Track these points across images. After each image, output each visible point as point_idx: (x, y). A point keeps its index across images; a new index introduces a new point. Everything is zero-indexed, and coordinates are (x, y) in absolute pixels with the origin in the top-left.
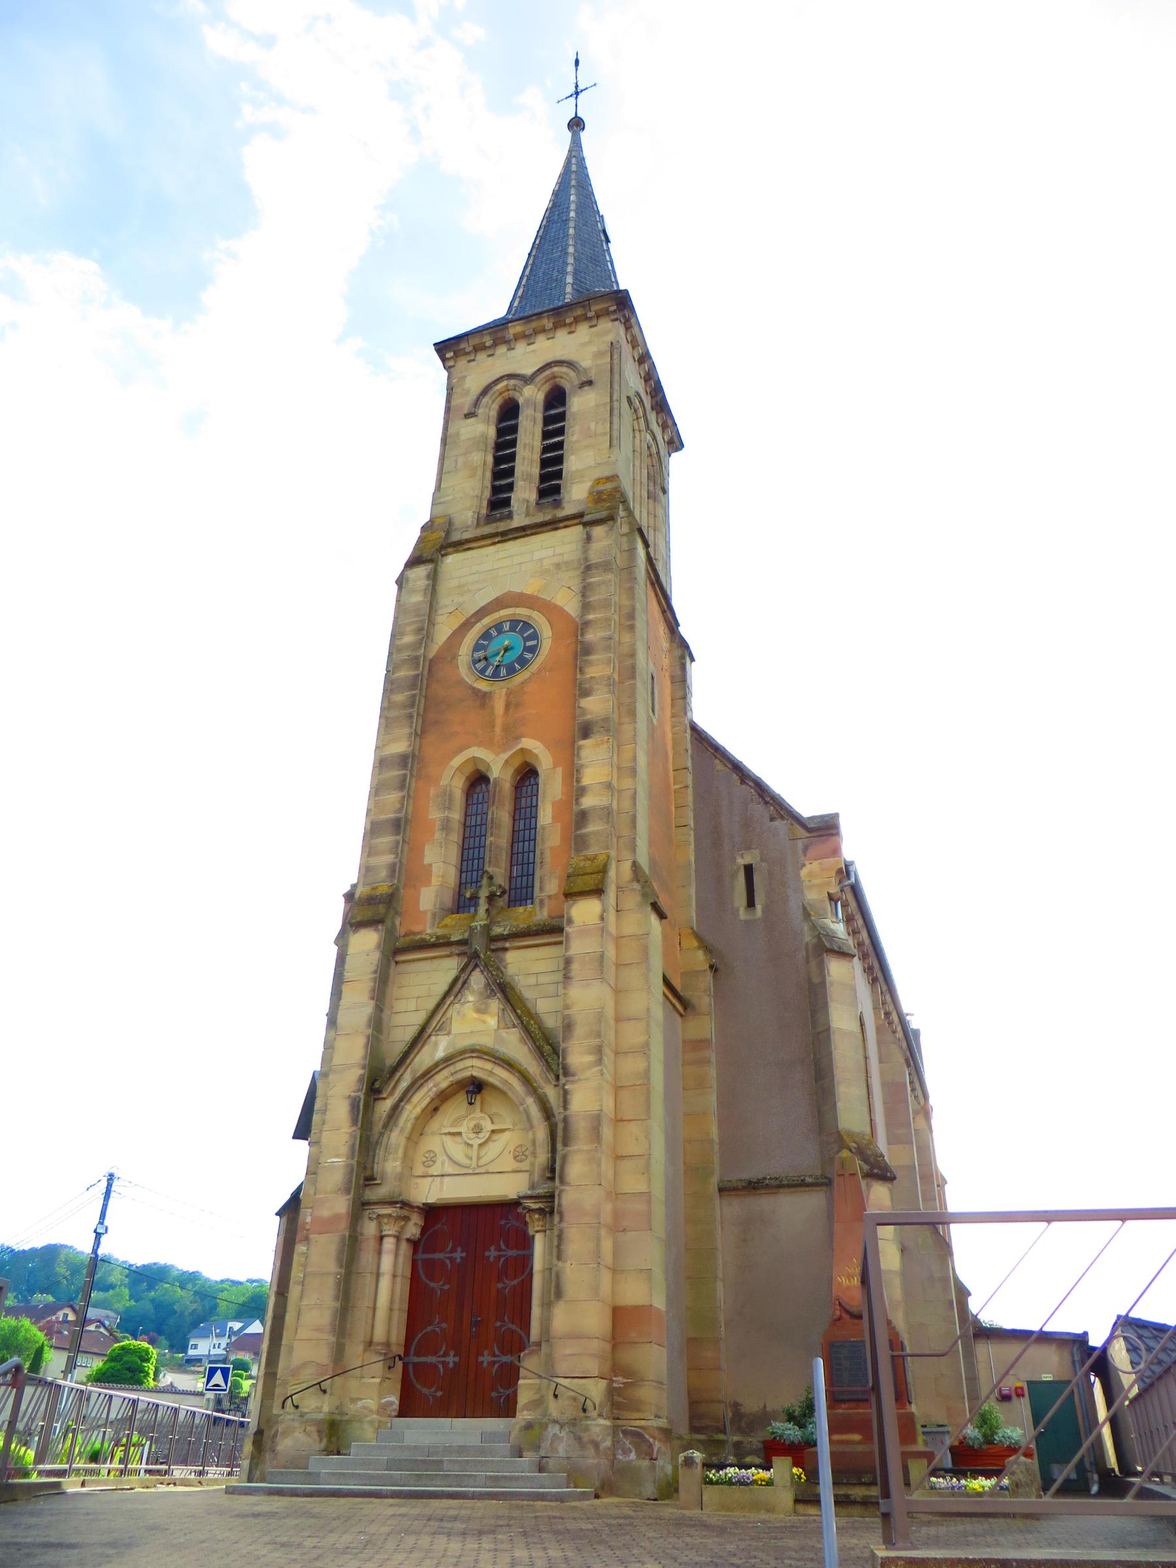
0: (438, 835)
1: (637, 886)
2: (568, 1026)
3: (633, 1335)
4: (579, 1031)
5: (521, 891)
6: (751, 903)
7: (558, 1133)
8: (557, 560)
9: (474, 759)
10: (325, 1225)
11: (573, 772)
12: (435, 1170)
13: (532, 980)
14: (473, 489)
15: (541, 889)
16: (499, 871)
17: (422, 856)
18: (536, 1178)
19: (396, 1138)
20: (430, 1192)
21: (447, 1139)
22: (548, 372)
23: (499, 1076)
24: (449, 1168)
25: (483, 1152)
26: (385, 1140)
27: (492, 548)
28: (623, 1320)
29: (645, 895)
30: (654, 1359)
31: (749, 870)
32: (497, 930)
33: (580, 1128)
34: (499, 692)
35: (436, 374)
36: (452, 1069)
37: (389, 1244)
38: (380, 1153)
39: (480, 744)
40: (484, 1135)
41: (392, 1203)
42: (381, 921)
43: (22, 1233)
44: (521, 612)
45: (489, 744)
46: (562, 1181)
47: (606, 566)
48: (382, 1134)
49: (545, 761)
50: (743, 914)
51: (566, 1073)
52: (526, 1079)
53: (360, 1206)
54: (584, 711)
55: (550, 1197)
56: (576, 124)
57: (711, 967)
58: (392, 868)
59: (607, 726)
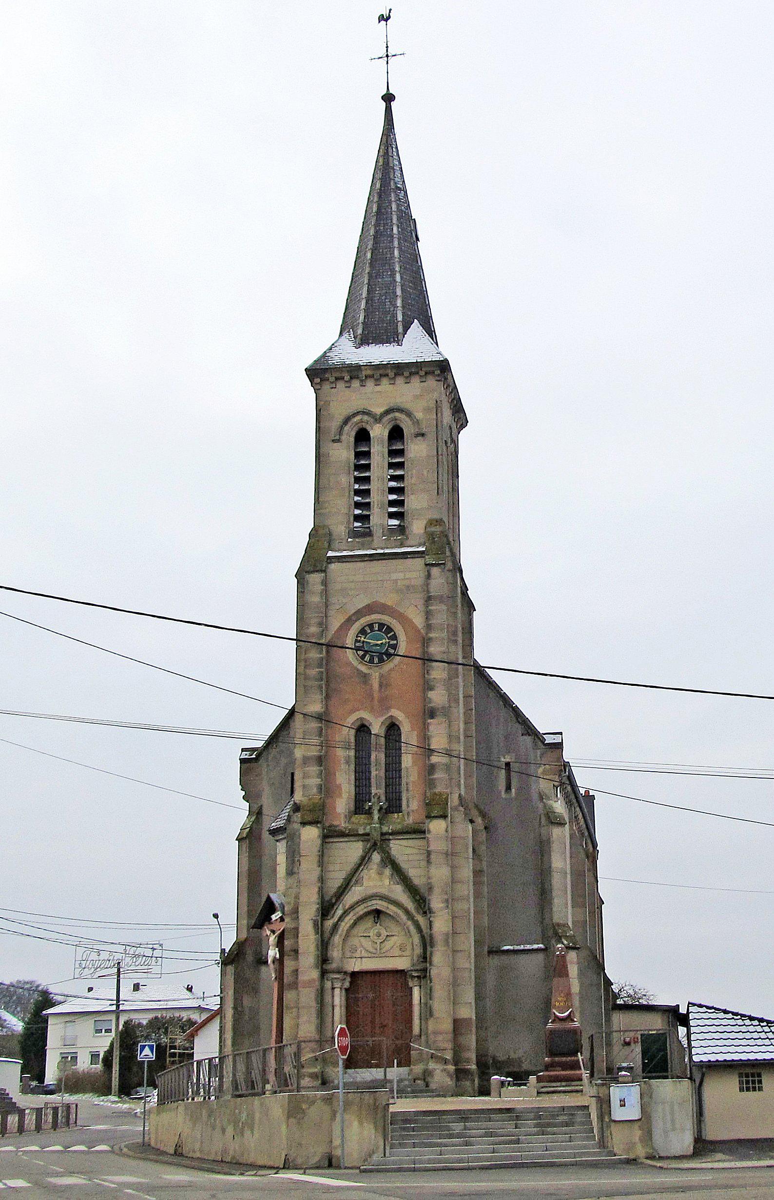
0: (343, 766)
1: (462, 809)
2: (430, 889)
3: (463, 1031)
4: (437, 891)
5: (393, 805)
6: (508, 788)
7: (427, 942)
8: (407, 582)
9: (361, 719)
10: (310, 982)
11: (425, 737)
12: (358, 955)
13: (406, 858)
14: (342, 505)
15: (408, 806)
16: (377, 789)
17: (335, 780)
18: (415, 959)
19: (337, 939)
20: (356, 966)
21: (362, 939)
22: (390, 416)
23: (392, 909)
24: (364, 954)
25: (383, 945)
26: (331, 942)
27: (363, 564)
28: (458, 1025)
29: (466, 814)
30: (471, 1040)
31: (508, 764)
32: (385, 829)
33: (439, 938)
34: (375, 674)
35: (305, 394)
36: (365, 905)
37: (337, 991)
38: (330, 948)
39: (365, 709)
40: (383, 937)
41: (339, 972)
42: (318, 822)
43: (8, 978)
44: (386, 619)
45: (372, 710)
46: (431, 964)
47: (441, 599)
48: (329, 939)
49: (406, 728)
50: (503, 795)
51: (430, 911)
52: (407, 912)
53: (324, 973)
54: (430, 701)
55: (425, 970)
56: (388, 98)
57: (486, 828)
58: (320, 787)
59: (446, 712)
